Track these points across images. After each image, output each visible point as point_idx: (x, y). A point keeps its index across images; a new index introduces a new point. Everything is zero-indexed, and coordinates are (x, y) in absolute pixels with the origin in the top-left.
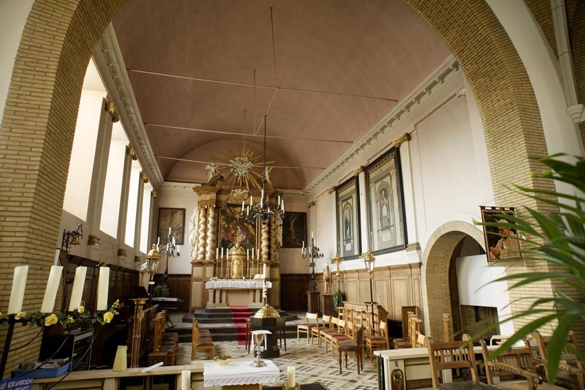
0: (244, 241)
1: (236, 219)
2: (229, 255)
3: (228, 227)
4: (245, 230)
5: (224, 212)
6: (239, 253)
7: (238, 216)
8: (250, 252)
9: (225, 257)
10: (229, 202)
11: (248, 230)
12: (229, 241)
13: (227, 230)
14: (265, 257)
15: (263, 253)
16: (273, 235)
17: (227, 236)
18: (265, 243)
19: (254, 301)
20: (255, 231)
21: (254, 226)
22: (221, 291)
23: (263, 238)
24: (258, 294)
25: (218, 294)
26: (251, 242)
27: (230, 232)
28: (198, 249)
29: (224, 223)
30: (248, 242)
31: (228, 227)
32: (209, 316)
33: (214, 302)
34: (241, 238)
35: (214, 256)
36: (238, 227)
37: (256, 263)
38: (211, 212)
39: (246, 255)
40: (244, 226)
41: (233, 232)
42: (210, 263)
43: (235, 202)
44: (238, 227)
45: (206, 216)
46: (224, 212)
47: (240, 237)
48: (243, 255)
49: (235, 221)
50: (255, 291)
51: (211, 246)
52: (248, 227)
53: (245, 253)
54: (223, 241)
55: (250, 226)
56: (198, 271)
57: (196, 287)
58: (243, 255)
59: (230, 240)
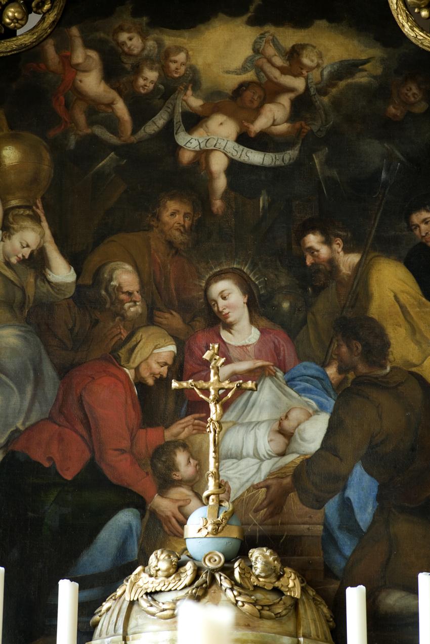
0: (308, 479)
1: (191, 180)
4: (319, 328)
27: (114, 358)
30: (361, 488)
31: (91, 294)
36: (229, 295)
41: (155, 353)
44: (229, 295)
49: (174, 214)
59: (121, 468)
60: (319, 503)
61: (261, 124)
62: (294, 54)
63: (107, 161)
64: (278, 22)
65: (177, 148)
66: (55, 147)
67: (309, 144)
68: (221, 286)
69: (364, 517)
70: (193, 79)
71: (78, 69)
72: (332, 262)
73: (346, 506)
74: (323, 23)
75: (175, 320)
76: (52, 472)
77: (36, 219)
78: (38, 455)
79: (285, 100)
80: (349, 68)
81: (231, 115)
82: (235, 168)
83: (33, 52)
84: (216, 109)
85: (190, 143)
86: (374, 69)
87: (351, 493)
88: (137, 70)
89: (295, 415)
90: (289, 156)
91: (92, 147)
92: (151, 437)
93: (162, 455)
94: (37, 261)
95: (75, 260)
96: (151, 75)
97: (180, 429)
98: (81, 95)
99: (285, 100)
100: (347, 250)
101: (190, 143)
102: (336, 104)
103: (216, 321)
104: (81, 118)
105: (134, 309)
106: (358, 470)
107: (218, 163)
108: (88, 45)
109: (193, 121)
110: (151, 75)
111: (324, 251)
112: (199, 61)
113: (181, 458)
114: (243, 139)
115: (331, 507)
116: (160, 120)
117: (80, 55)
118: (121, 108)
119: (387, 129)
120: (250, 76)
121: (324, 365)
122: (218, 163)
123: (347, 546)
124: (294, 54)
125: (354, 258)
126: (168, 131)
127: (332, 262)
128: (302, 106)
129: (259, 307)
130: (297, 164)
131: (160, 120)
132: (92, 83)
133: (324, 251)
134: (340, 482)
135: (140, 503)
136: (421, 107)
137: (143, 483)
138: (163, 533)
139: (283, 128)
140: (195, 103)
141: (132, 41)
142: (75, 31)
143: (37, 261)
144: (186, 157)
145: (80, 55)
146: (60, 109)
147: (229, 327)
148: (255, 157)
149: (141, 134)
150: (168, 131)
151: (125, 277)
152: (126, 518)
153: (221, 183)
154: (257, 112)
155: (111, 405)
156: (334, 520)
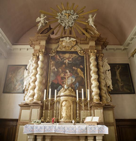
0: (73, 83)
1: (65, 64)
3: (58, 71)
4: (74, 73)
5: (53, 58)
7: (67, 61)
9: (52, 100)
10: (59, 49)
11: (77, 73)
12: (58, 83)
13: (57, 74)
14: (96, 98)
15: (93, 94)
16: (103, 78)
17: (56, 79)
18: (94, 84)
20: (84, 74)
21: (83, 70)
23: (92, 79)
26: (82, 83)
27: (59, 75)
29: (54, 67)
30: (77, 84)
31: (58, 71)
34: (70, 81)
35: (41, 98)
36: (68, 71)
37: (86, 105)
38: (41, 57)
39: (76, 97)
40: (73, 70)
41: (62, 75)
43: (64, 50)
44: (68, 71)
47: (70, 80)
48: (72, 96)
49: (64, 66)
51: (39, 88)
52: (77, 70)
53: (74, 95)
54: (53, 84)
55: (79, 70)
56: (26, 113)
58: (72, 96)
59: (60, 83)
60: (74, 85)
61: (69, 60)
62: (72, 56)
63: (59, 62)
64: (71, 54)
65: (64, 62)
67: (73, 61)
69: (78, 86)
70: (65, 57)
71: (57, 57)
72: (75, 69)
73: (76, 85)
74: (74, 54)
75: (64, 73)
76: (55, 83)
77: (54, 66)
79: (71, 58)
81: (68, 59)
82: (68, 63)
84: (67, 59)
85: (65, 61)
86: (77, 56)
87: (77, 84)
88: (61, 57)
89: (73, 79)
90: (72, 62)
91: (58, 62)
92: (62, 81)
93: (63, 82)
94: (54, 69)
95: (57, 69)
96: (62, 57)
97: (64, 80)
98: (58, 58)
99: (71, 58)
100: (76, 68)
101: (65, 61)
102: (75, 59)
103: (67, 73)
104: (57, 60)
105: (61, 72)
106: (77, 83)
107: (67, 62)
108: (58, 55)
109: (65, 60)
110: (62, 57)
111: (74, 68)
113: (64, 82)
114: (68, 61)
115: (75, 85)
116: (63, 60)
118: (60, 59)
119: (78, 60)
120: (69, 57)
121: (74, 76)
122: (67, 62)
123: (76, 88)
124: (72, 56)
125: (76, 68)
126: (63, 61)
127: (75, 69)
128: (72, 59)
129: (70, 72)
130: (73, 62)
131: (63, 60)
132: (58, 58)
133: (74, 68)
134: (76, 84)
135: (61, 85)
136: (80, 59)
137: (61, 84)
139: (71, 60)
140: (65, 59)
141: (61, 55)
142: (57, 55)
143: (54, 69)
144: (64, 62)
146: (56, 59)
147: (68, 73)
148: (69, 62)
149: (62, 61)
150: (63, 61)
151: (60, 70)
152: (60, 86)
153: (67, 64)
154: (69, 59)
155: (59, 78)
156: (75, 86)
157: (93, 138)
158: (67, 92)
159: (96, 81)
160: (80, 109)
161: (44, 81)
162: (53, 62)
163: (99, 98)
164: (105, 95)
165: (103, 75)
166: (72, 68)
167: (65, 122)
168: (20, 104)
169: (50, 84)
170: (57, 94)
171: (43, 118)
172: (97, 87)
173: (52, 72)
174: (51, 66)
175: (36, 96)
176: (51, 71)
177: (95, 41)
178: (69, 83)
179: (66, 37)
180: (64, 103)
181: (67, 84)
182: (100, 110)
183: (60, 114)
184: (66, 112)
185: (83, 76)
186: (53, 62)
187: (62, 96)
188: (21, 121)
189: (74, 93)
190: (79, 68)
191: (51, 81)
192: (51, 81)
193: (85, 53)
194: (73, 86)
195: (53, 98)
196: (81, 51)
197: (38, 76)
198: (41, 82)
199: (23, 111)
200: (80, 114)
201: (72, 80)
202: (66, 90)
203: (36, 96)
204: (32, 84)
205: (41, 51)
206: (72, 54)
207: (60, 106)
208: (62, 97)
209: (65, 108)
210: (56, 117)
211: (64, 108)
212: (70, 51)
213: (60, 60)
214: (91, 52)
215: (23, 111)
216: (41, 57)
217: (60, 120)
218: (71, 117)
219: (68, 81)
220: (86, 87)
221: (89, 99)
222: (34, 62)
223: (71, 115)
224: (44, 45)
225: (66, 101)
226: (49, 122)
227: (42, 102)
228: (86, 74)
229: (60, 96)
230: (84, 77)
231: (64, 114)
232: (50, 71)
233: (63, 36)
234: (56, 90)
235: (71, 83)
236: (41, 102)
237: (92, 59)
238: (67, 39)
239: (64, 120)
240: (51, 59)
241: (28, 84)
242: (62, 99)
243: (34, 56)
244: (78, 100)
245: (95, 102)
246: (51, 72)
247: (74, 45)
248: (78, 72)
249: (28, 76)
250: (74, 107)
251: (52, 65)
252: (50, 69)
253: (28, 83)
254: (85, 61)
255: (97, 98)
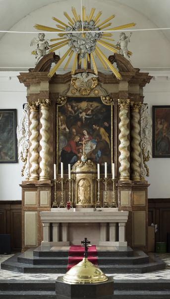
1: (81, 119)
2: (72, 173)
3: (70, 132)
5: (63, 110)
6: (86, 170)
7: (83, 115)
8: (102, 168)
9: (66, 176)
10: (69, 94)
11: (99, 136)
12: (71, 152)
13: (69, 137)
14: (124, 175)
15: (121, 169)
16: (138, 142)
17: (69, 145)
18: (123, 154)
19: (108, 240)
21: (108, 130)
22: (60, 225)
23: (121, 146)
24: (112, 231)
25: (55, 230)
26: (106, 153)
27: (73, 139)
28: (30, 166)
29: (64, 126)
30: (99, 153)
31: (70, 132)
32: (35, 262)
33: (51, 239)
34: (89, 148)
35: (50, 175)
36: (85, 132)
37: (110, 184)
38: (43, 111)
39: (97, 173)
40: (94, 130)
42: (44, 186)
43: (78, 94)
44: (85, 132)
45: (37, 117)
46: (63, 110)
47: (88, 147)
49: (79, 123)
50: (108, 225)
51: (46, 161)
53: (94, 171)
55: (102, 130)
56: (31, 197)
57: (29, 219)
59: (74, 151)
61: (88, 113)
62: (91, 105)
63: (72, 118)
65: (79, 116)
66: (66, 116)
68: (84, 131)
69: (100, 156)
70: (81, 108)
75: (79, 135)
78: (66, 150)
80: (97, 107)
82: (85, 118)
83: (64, 106)
85: (81, 115)
90: (91, 117)
91: (70, 116)
92: (78, 148)
93: (79, 149)
94: (65, 129)
95: (68, 129)
96: (76, 108)
101: (81, 115)
103: (84, 135)
104: (69, 113)
106: (99, 151)
107: (84, 118)
109: (81, 113)
110: (76, 108)
112: (82, 106)
114: (86, 115)
115: (96, 154)
116: (77, 113)
117: (68, 106)
122: (84, 118)
123: (98, 159)
124: (91, 105)
126: (78, 114)
128: (92, 111)
129: (88, 133)
130: (92, 117)
131: (77, 113)
132: (70, 109)
135: (76, 155)
136: (105, 111)
137: (77, 153)
138: (79, 158)
140: (81, 111)
141: (74, 104)
143: (65, 129)
145: (68, 106)
148: (88, 117)
150: (78, 114)
151: (74, 130)
152: (75, 157)
153: (84, 120)
155: (73, 145)
157: (115, 225)
158: (85, 168)
159: (125, 150)
160: (102, 189)
161: (52, 150)
162: (62, 117)
163: (129, 175)
164: (138, 169)
165: (138, 137)
166: (92, 127)
167: (83, 207)
168: (21, 184)
169: (62, 155)
170: (71, 169)
171: (54, 202)
172: (127, 159)
173: (62, 134)
174: (60, 124)
175: (42, 174)
176: (60, 132)
177: (128, 82)
178: (87, 152)
179: (82, 73)
180: (81, 183)
181: (85, 153)
182: (127, 192)
183: (76, 196)
184: (85, 193)
185: (107, 140)
186: (62, 117)
187: (78, 173)
188: (25, 206)
189: (94, 167)
190: (102, 126)
191: (61, 148)
192: (61, 148)
193: (113, 100)
194: (94, 156)
195: (67, 175)
196: (106, 98)
197: (42, 143)
198: (49, 153)
199: (26, 193)
200: (102, 196)
201: (91, 147)
202: (83, 164)
203: (42, 174)
204: (34, 154)
205: (43, 101)
206: (92, 102)
207: (76, 186)
208: (77, 175)
209: (83, 188)
210: (71, 200)
211: (81, 189)
212: (89, 96)
213: (73, 114)
214: (122, 103)
215: (26, 193)
216: (43, 111)
217: (77, 204)
218: (90, 200)
219: (86, 148)
220: (112, 157)
221: (113, 178)
222: (31, 115)
223: (90, 198)
224: (46, 91)
225: (84, 179)
226: (63, 207)
227: (53, 182)
228: (112, 138)
229: (75, 173)
230: (108, 142)
231: (81, 197)
232: (58, 133)
233: (77, 72)
234: (69, 165)
235: (91, 151)
236: (51, 183)
237: (123, 113)
238: (84, 77)
239: (82, 204)
240: (59, 111)
241: (26, 151)
242: (78, 176)
243: (31, 105)
244: (99, 178)
245: (122, 181)
246: (61, 135)
247: (94, 86)
248: (101, 133)
249: (24, 137)
250: (94, 186)
251: (61, 122)
252: (59, 128)
253: (25, 149)
254: (112, 115)
255: (126, 175)
